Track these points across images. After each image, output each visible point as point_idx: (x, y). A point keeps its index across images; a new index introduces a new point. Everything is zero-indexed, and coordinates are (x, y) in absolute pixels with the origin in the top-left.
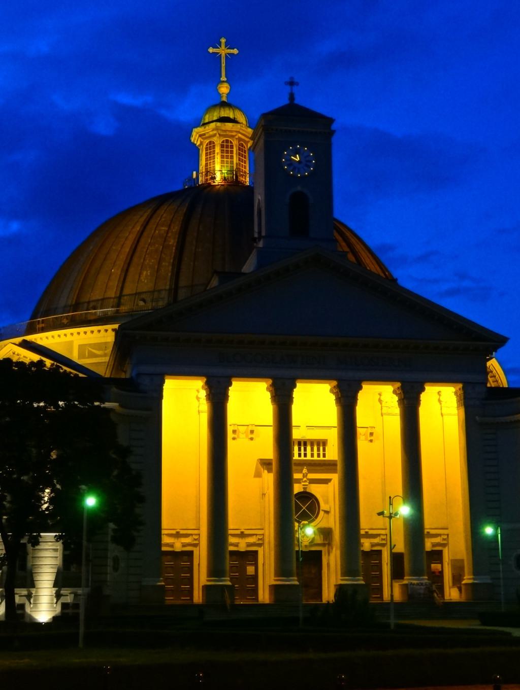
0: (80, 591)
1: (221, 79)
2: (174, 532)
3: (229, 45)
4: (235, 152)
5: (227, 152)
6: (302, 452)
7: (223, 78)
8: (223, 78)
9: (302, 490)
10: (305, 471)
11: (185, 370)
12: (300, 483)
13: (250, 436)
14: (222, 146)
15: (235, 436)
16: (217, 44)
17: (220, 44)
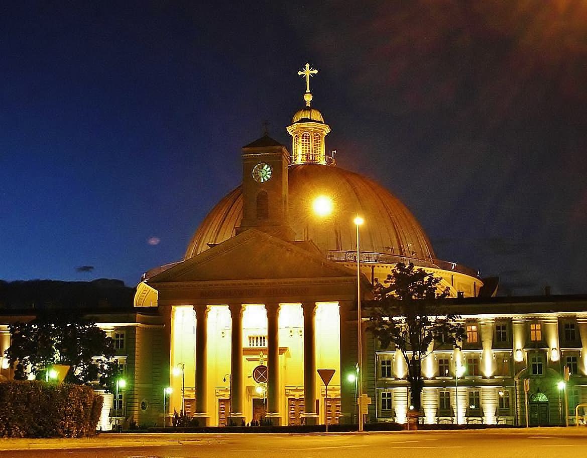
0: (121, 419)
1: (307, 91)
2: (190, 389)
3: (313, 67)
4: (311, 141)
5: (306, 141)
6: (262, 343)
7: (308, 91)
8: (308, 91)
9: (260, 365)
10: (261, 354)
11: (183, 300)
12: (259, 361)
13: (223, 335)
14: (303, 138)
15: (224, 335)
16: (302, 68)
17: (305, 68)
